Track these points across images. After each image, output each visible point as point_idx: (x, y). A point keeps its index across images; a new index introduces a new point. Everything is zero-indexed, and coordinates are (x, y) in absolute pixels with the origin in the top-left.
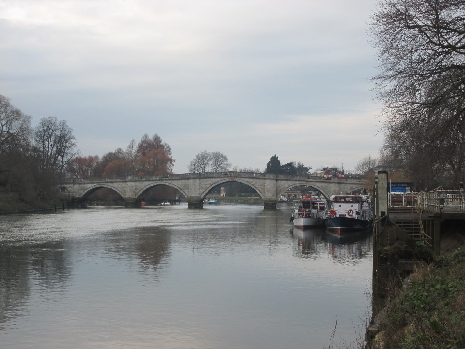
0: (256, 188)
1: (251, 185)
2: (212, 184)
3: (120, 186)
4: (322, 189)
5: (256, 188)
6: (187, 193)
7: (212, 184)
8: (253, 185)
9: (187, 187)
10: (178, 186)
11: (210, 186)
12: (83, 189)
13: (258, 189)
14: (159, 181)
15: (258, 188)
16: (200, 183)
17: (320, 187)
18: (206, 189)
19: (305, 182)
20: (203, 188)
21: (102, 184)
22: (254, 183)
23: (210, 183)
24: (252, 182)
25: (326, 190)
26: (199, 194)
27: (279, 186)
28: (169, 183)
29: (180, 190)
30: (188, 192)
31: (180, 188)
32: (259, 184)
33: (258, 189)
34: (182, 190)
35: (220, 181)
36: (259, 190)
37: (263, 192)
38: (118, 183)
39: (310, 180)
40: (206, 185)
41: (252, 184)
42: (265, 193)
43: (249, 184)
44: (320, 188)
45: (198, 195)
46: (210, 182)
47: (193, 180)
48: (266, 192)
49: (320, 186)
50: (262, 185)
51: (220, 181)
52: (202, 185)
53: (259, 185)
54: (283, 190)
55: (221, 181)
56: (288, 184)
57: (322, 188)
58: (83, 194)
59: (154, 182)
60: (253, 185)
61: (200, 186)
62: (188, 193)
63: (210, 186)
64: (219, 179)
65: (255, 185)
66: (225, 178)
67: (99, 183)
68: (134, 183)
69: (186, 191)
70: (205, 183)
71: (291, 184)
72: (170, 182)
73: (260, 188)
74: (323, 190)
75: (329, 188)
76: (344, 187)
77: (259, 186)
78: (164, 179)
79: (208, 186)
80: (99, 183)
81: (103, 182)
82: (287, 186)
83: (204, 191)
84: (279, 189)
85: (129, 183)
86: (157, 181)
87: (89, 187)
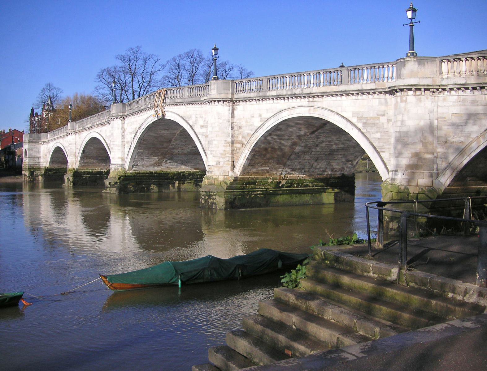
17: (354, 120)
19: (304, 102)
20: (128, 142)
23: (136, 128)
25: (378, 135)
26: (119, 158)
27: (240, 127)
32: (201, 122)
39: (322, 89)
44: (351, 122)
45: (120, 162)
49: (355, 114)
52: (127, 135)
53: (202, 126)
56: (260, 115)
57: (360, 125)
61: (123, 137)
70: (131, 131)
74: (363, 133)
75: (389, 121)
77: (204, 130)
82: (257, 123)
84: (240, 139)
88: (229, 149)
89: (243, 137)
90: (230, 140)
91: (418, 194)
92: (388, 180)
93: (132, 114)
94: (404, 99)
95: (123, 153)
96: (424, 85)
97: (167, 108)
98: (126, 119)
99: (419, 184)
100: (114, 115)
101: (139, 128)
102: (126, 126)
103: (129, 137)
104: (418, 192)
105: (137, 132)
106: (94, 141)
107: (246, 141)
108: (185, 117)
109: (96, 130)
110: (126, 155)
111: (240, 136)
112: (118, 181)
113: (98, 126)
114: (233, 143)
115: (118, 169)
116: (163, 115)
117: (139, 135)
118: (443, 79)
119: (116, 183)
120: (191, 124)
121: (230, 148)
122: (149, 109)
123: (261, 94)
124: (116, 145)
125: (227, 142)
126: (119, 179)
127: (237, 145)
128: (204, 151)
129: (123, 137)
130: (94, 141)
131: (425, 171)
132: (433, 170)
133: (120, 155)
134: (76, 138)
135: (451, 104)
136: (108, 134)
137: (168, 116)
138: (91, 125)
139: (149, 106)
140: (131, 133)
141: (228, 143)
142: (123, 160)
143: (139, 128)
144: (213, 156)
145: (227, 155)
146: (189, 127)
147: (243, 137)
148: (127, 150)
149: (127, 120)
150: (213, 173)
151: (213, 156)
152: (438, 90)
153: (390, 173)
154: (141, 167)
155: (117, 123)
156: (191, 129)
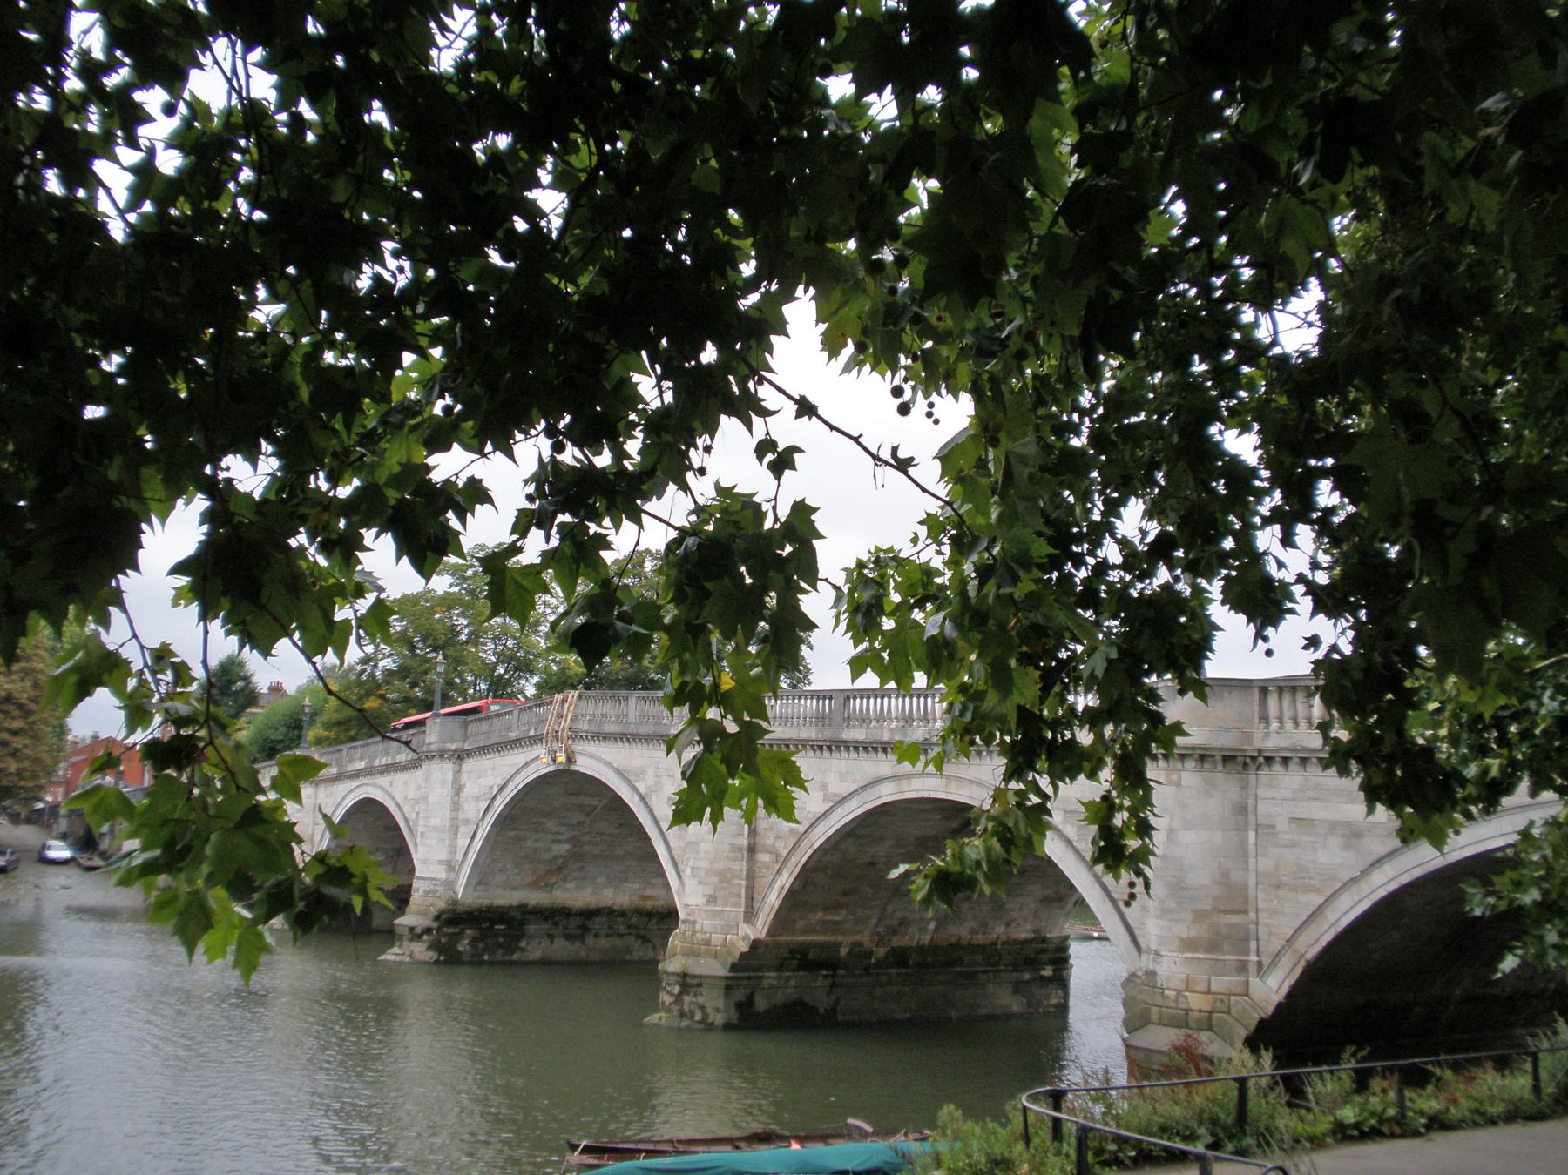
4: (1069, 842)
7: (495, 797)
8: (642, 798)
10: (406, 809)
11: (487, 810)
16: (458, 789)
20: (467, 821)
23: (491, 787)
24: (642, 772)
26: (440, 862)
45: (441, 874)
51: (518, 771)
54: (792, 841)
55: (527, 765)
59: (354, 784)
60: (646, 804)
61: (456, 807)
65: (653, 802)
70: (476, 791)
71: (843, 789)
76: (1302, 811)
84: (769, 841)
88: (742, 866)
89: (777, 838)
90: (744, 842)
91: (1210, 1012)
92: (1139, 973)
93: (483, 750)
94: (1174, 777)
95: (453, 850)
96: (1221, 749)
97: (580, 747)
98: (466, 760)
99: (1213, 988)
100: (433, 747)
101: (502, 788)
102: (464, 778)
103: (472, 809)
104: (1209, 1009)
105: (495, 797)
106: (369, 809)
107: (785, 848)
108: (628, 771)
110: (459, 857)
111: (771, 834)
112: (435, 925)
113: (385, 769)
114: (752, 850)
115: (435, 892)
116: (570, 760)
117: (499, 805)
118: (1267, 735)
119: (428, 930)
120: (642, 790)
121: (744, 863)
122: (537, 740)
123: (828, 734)
124: (434, 827)
125: (736, 848)
126: (437, 918)
127: (763, 857)
128: (675, 864)
129: (456, 807)
130: (369, 809)
131: (1227, 957)
132: (1247, 953)
133: (444, 856)
134: (316, 794)
135: (1288, 794)
136: (412, 795)
137: (583, 765)
138: (362, 765)
139: (532, 733)
140: (478, 798)
141: (740, 849)
142: (451, 866)
143: (502, 788)
144: (700, 883)
145: (736, 881)
146: (636, 798)
147: (777, 838)
148: (462, 842)
149: (469, 765)
150: (698, 927)
151: (700, 883)
152: (1253, 759)
153: (1144, 956)
154: (498, 891)
155: (441, 771)
156: (642, 805)
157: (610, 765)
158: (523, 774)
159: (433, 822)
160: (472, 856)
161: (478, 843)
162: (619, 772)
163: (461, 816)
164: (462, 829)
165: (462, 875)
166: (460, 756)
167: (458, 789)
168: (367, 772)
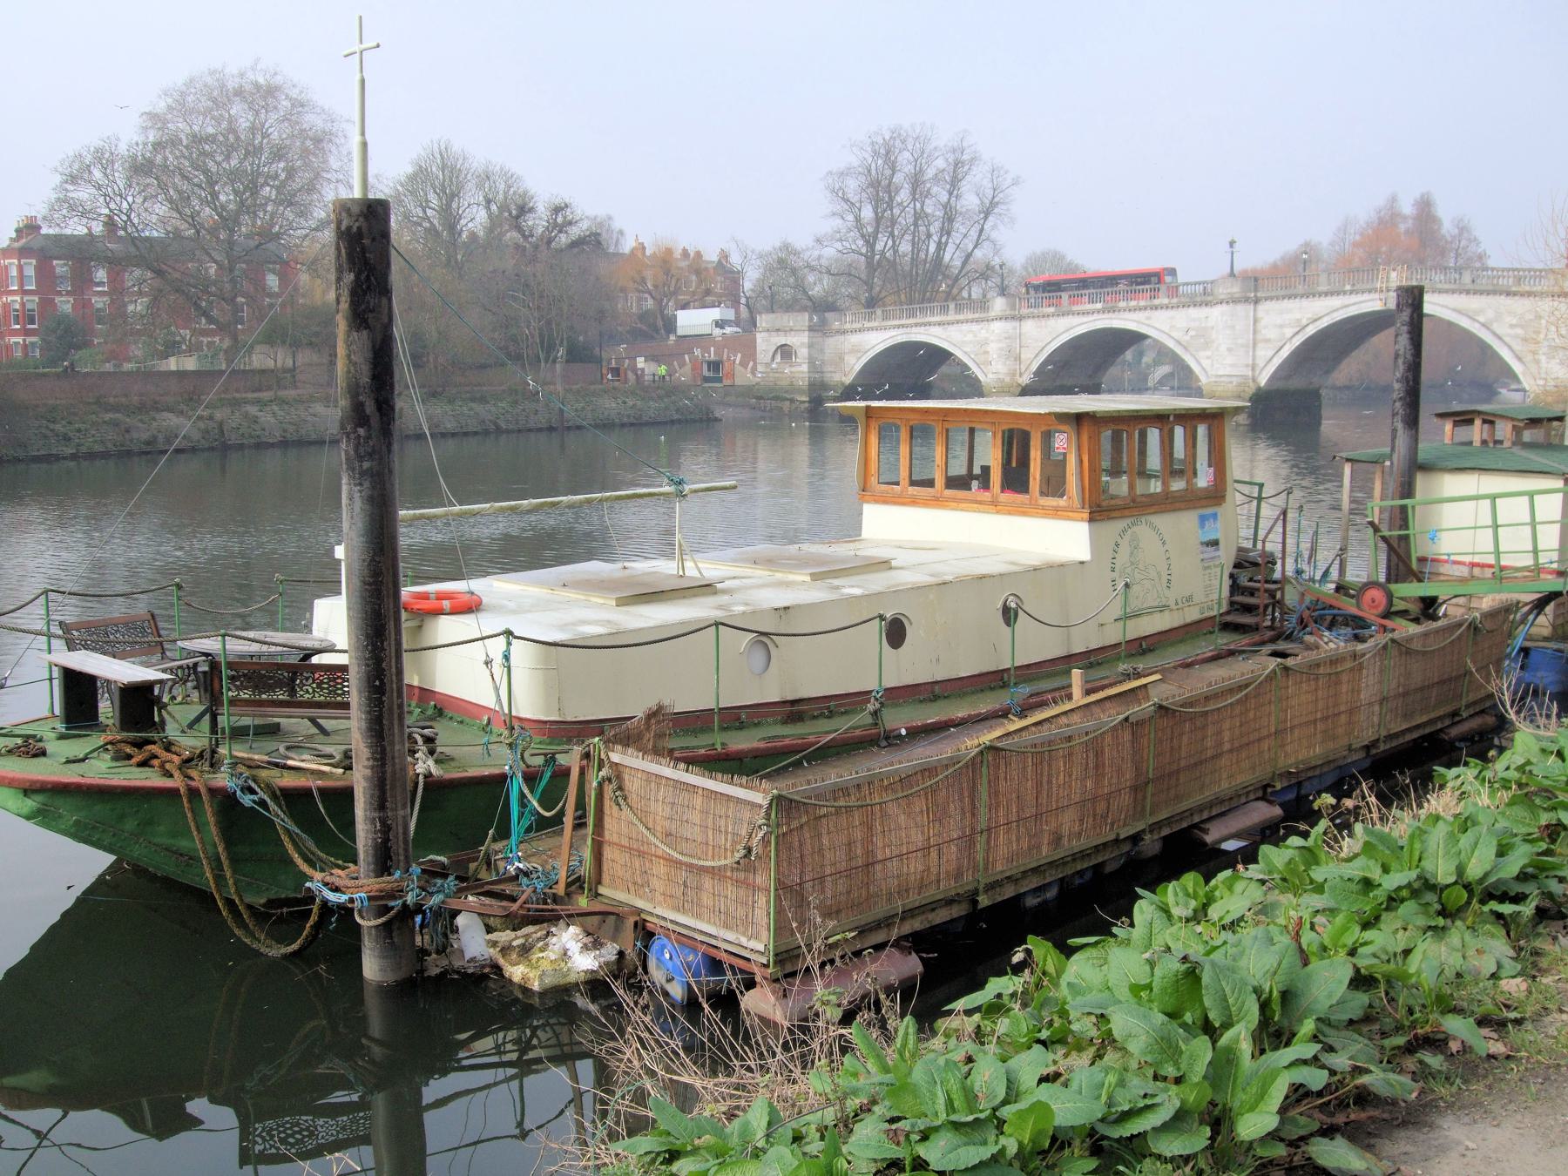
0: (1499, 338)
1: (1477, 325)
2: (1304, 322)
3: (970, 337)
5: (1499, 338)
6: (1206, 363)
8: (1483, 325)
9: (1203, 337)
10: (1174, 334)
11: (1297, 333)
12: (859, 351)
13: (1506, 344)
14: (1106, 316)
15: (1507, 339)
16: (1256, 321)
18: (1280, 344)
20: (1267, 341)
21: (914, 330)
22: (1490, 314)
23: (1299, 320)
26: (1247, 366)
28: (1138, 322)
29: (1179, 351)
30: (1208, 358)
31: (1179, 342)
32: (1514, 322)
33: (1506, 344)
34: (1185, 348)
35: (1337, 310)
36: (1510, 348)
37: (1529, 358)
38: (965, 327)
40: (1281, 326)
41: (1482, 319)
42: (1538, 362)
43: (1465, 323)
46: (1298, 316)
47: (1224, 307)
48: (1543, 358)
50: (1522, 327)
51: (1337, 310)
53: (1512, 326)
58: (858, 368)
60: (1488, 328)
61: (1255, 332)
62: (1209, 362)
63: (1297, 333)
64: (1335, 302)
65: (1495, 327)
66: (1359, 298)
67: (903, 326)
68: (1016, 324)
69: (1202, 354)
72: (1141, 316)
73: (1516, 336)
77: (1519, 331)
78: (1122, 304)
79: (1289, 332)
80: (903, 326)
81: (916, 325)
83: (1271, 353)
85: (997, 326)
86: (1101, 316)
87: (875, 342)
102: (1260, 314)
109: (1127, 315)
117: (1311, 331)
128: (1519, 359)
142: (1253, 369)
148: (1263, 353)
157: (1446, 307)
158: (1341, 312)
159: (1240, 341)
160: (1277, 361)
161: (1285, 353)
162: (1454, 310)
163: (1259, 337)
164: (1260, 345)
165: (1264, 373)
166: (1257, 301)
167: (1256, 321)
168: (1113, 310)
